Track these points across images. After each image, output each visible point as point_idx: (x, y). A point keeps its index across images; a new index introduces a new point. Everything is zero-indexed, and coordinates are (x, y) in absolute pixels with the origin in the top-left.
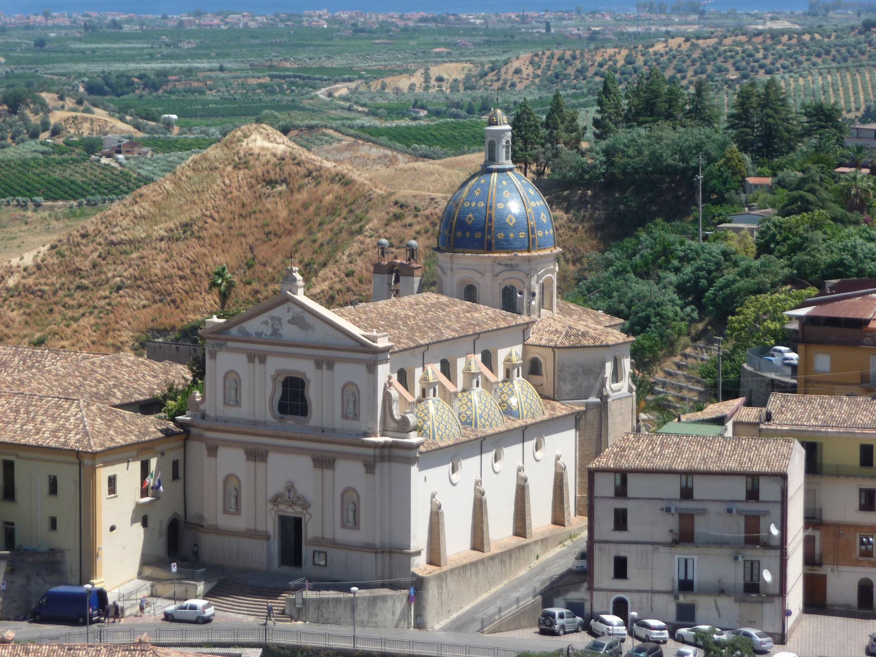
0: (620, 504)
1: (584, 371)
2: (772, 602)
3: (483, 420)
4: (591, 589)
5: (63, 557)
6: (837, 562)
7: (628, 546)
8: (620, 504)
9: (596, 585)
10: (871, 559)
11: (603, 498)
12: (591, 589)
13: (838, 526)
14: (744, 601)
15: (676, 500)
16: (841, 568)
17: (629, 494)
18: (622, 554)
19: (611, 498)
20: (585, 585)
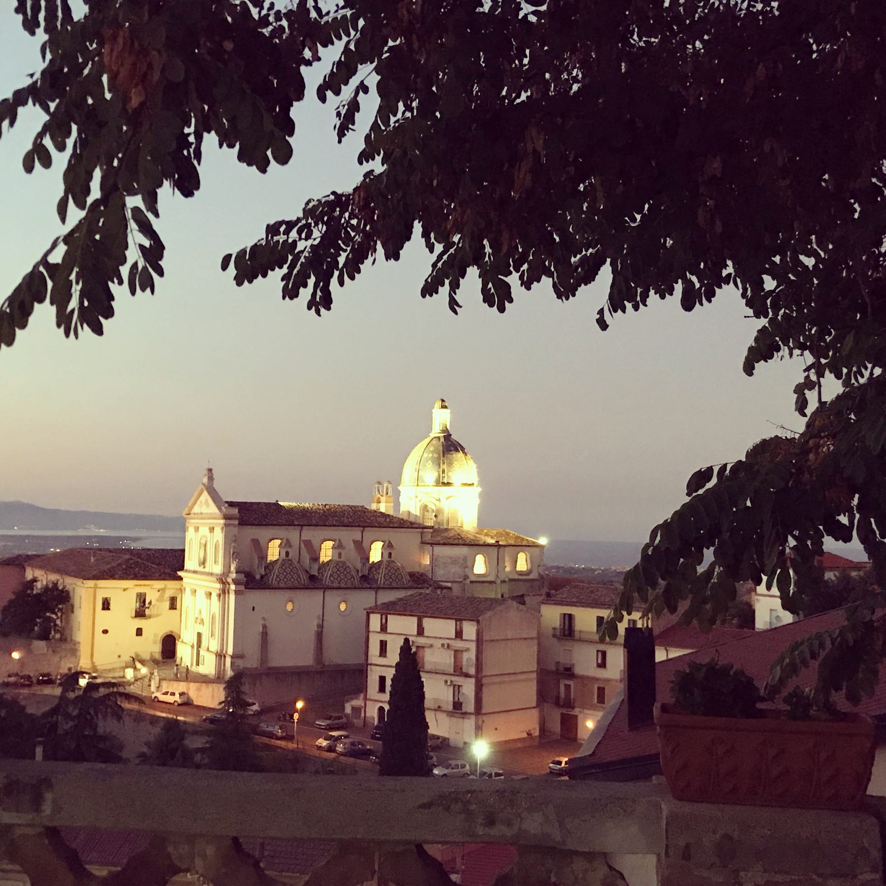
0: (383, 637)
1: (452, 562)
2: (469, 718)
3: (332, 579)
4: (366, 699)
5: (79, 647)
6: (583, 707)
7: (386, 668)
8: (383, 637)
9: (368, 697)
10: (603, 705)
11: (374, 632)
12: (366, 699)
13: (583, 678)
14: (452, 716)
15: (414, 636)
16: (586, 711)
17: (389, 631)
18: (383, 675)
19: (378, 632)
20: (362, 696)
